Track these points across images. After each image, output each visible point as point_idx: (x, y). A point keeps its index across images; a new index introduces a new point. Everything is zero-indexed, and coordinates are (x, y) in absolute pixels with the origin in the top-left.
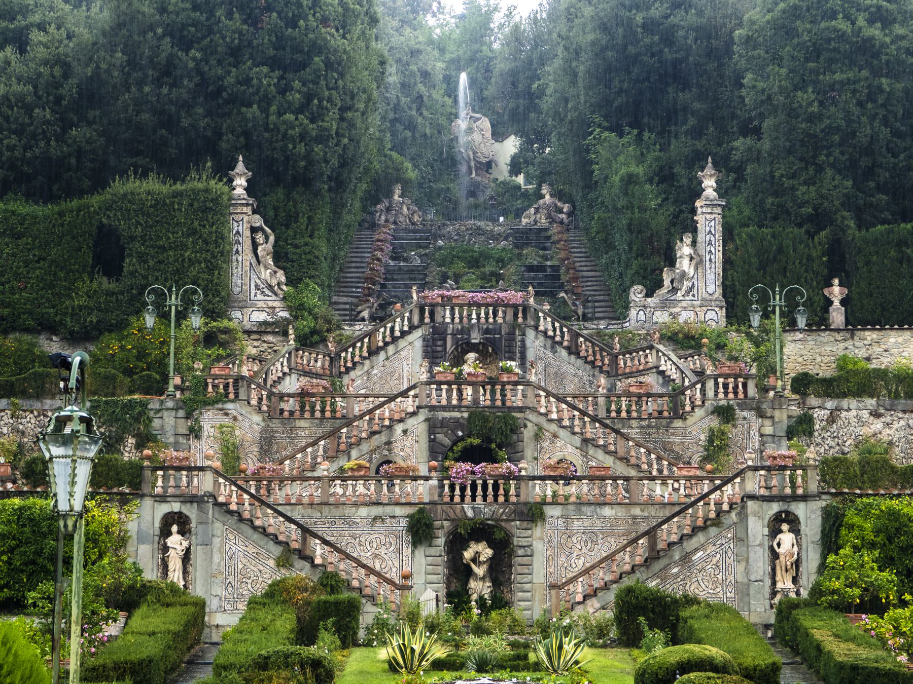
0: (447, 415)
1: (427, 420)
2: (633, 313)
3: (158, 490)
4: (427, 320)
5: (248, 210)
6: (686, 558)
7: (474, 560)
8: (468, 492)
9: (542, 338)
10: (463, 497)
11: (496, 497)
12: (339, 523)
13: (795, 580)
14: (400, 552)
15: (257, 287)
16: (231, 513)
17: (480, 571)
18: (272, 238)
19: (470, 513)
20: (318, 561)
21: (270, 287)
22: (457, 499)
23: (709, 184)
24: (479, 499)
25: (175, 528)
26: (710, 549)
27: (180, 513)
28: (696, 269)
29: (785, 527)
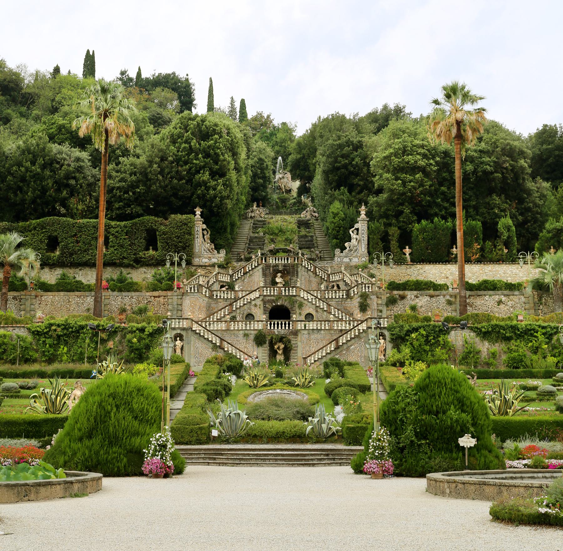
0: (269, 298)
1: (263, 300)
2: (336, 258)
3: (173, 326)
4: (264, 262)
5: (201, 223)
6: (348, 348)
7: (278, 348)
8: (276, 326)
9: (303, 268)
10: (274, 327)
11: (285, 327)
12: (233, 336)
13: (384, 355)
14: (253, 346)
15: (204, 250)
16: (197, 333)
17: (280, 352)
18: (209, 232)
19: (277, 333)
20: (226, 349)
21: (209, 250)
22: (272, 328)
23: (363, 213)
24: (280, 328)
25: (178, 339)
26: (356, 345)
27: (180, 334)
28: (358, 243)
29: (381, 337)
